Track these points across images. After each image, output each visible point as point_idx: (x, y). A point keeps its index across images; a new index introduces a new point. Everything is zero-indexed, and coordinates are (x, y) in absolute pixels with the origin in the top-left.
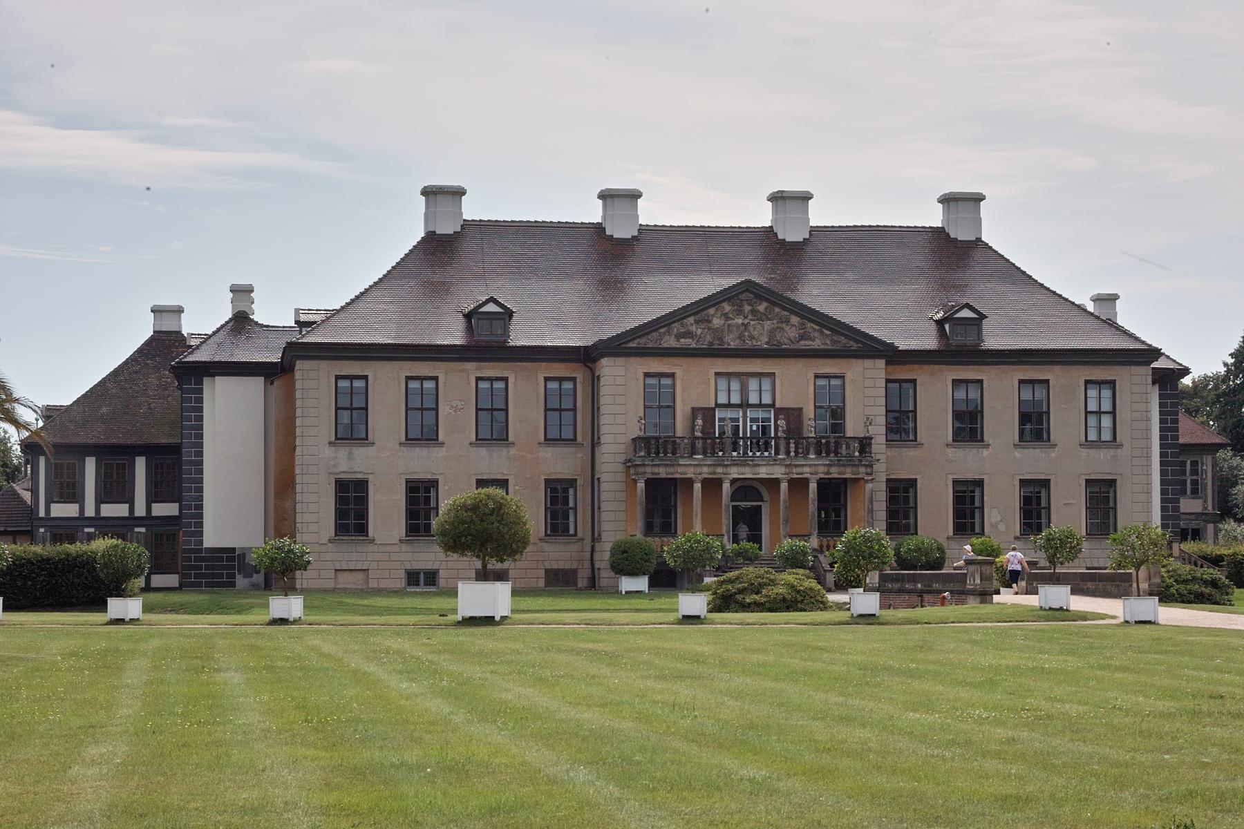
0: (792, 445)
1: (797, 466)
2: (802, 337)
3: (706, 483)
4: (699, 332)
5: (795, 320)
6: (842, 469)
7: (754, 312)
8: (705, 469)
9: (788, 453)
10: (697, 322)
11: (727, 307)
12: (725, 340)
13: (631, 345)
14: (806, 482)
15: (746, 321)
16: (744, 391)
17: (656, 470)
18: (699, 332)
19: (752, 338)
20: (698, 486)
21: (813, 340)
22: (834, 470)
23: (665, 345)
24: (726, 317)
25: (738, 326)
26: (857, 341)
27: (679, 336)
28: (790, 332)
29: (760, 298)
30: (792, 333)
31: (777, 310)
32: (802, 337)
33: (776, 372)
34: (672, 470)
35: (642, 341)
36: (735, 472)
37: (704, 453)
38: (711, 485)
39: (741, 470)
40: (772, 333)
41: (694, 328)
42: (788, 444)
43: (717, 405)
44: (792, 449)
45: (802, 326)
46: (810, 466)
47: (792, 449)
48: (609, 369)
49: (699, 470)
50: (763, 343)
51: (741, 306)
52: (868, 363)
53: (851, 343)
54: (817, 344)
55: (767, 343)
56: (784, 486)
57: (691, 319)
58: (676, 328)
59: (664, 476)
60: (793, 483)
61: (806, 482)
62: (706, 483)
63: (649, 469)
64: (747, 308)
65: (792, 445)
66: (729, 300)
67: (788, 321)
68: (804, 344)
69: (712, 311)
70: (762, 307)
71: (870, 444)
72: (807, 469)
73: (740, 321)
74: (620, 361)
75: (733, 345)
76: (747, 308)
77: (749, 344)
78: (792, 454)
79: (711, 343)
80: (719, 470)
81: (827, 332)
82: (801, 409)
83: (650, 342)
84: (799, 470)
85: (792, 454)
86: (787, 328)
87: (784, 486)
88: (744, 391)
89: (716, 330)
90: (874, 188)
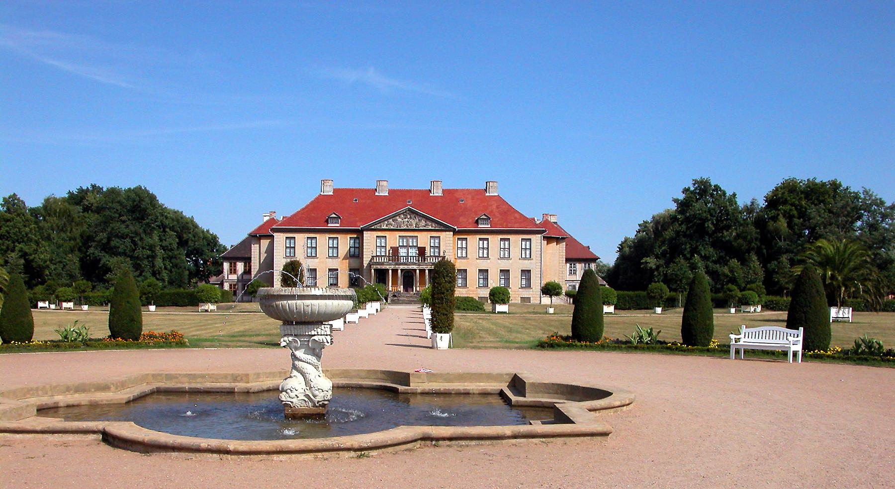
16: (407, 241)
36: (402, 267)
38: (395, 271)
83: (378, 227)
88: (407, 241)
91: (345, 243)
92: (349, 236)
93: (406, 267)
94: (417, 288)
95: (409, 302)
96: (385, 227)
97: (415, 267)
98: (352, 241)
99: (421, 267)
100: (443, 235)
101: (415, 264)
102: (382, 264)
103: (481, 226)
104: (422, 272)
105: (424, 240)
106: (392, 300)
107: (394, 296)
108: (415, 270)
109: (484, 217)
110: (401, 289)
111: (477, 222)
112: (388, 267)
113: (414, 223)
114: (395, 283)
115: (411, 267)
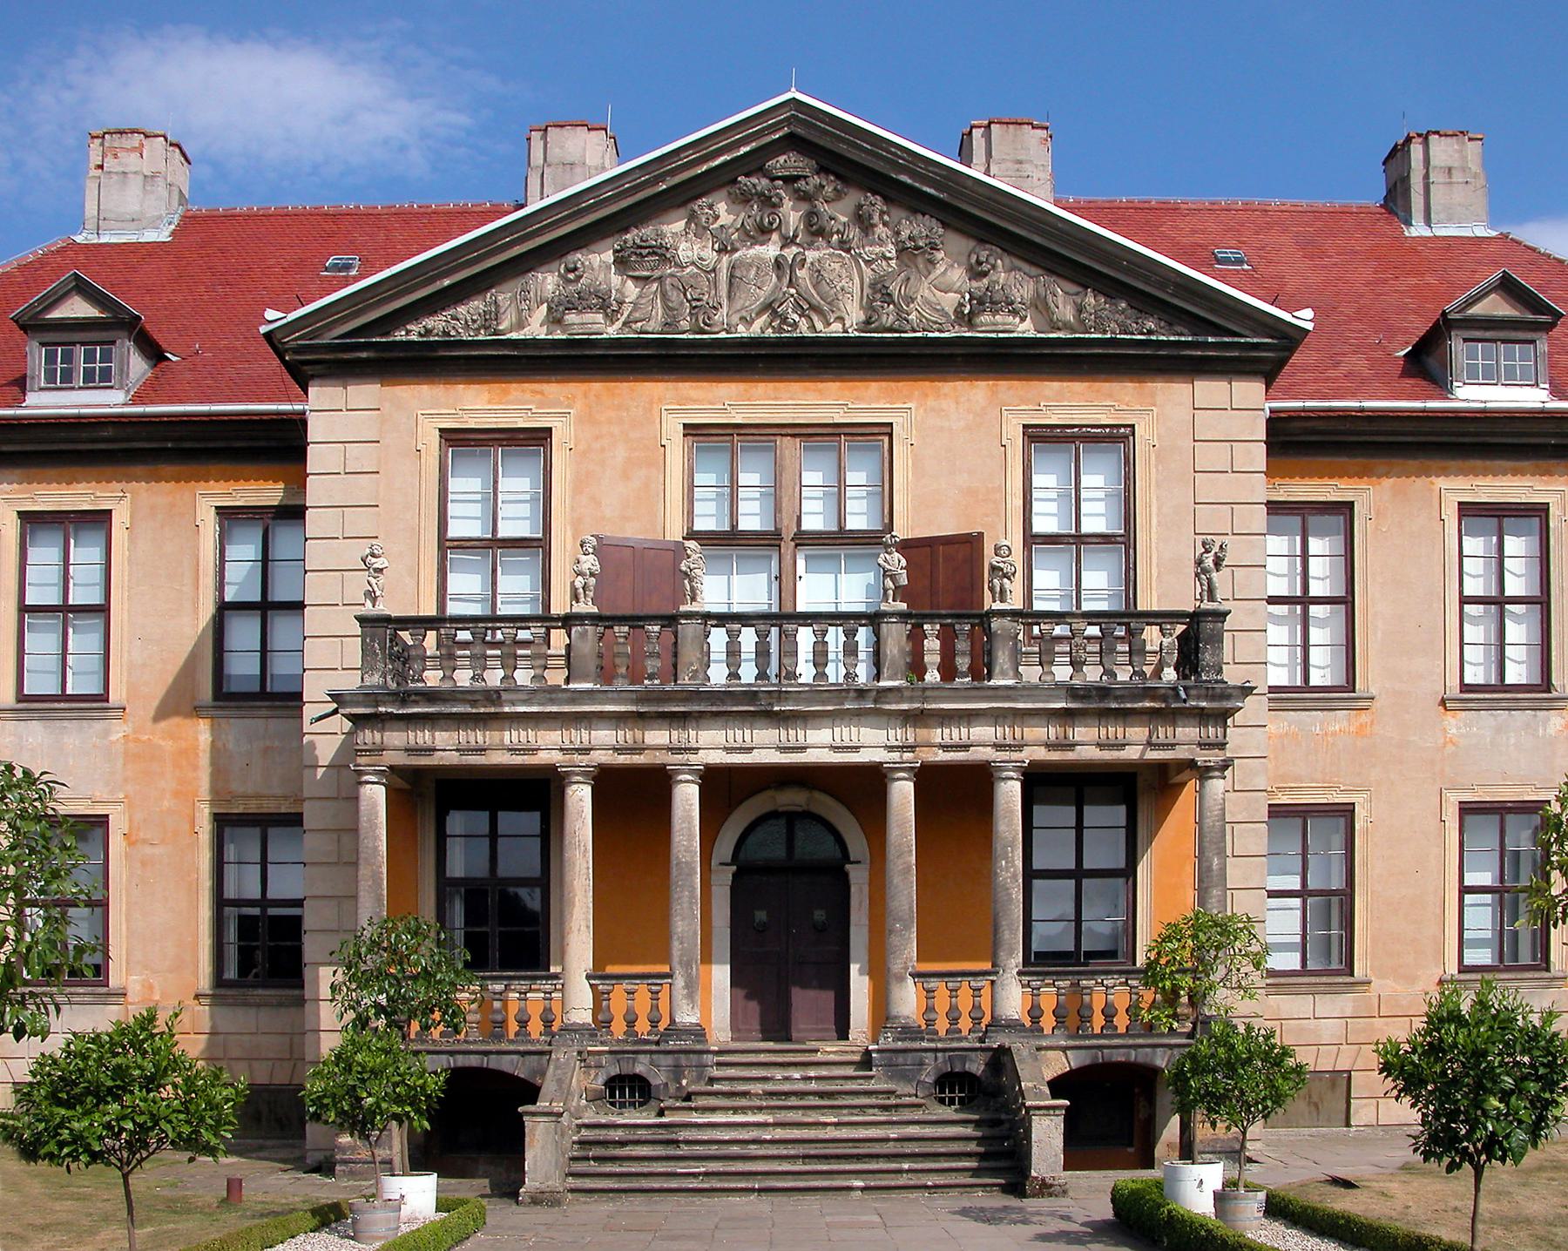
0: (932, 644)
1: (947, 718)
2: (981, 302)
3: (608, 782)
6: (1113, 731)
8: (604, 736)
9: (917, 667)
11: (724, 212)
13: (400, 336)
14: (980, 778)
16: (779, 493)
17: (423, 737)
20: (580, 797)
22: (1081, 733)
28: (939, 293)
33: (897, 421)
34: (479, 737)
36: (714, 745)
37: (605, 673)
38: (632, 798)
39: (740, 735)
42: (916, 637)
43: (692, 535)
44: (932, 658)
46: (996, 717)
47: (932, 658)
48: (337, 415)
49: (580, 736)
52: (1210, 390)
56: (903, 793)
59: (453, 758)
60: (929, 779)
61: (980, 778)
62: (608, 782)
63: (396, 737)
65: (932, 644)
71: (1217, 639)
72: (983, 732)
74: (365, 393)
78: (933, 676)
80: (657, 736)
82: (972, 542)
83: (459, 322)
84: (955, 734)
85: (933, 676)
87: (903, 793)
88: (779, 493)
91: (165, 553)
92: (206, 498)
93: (764, 746)
94: (896, 989)
95: (824, 1169)
96: (536, 328)
97: (871, 744)
98: (245, 551)
99: (941, 745)
100: (1164, 412)
101: (860, 704)
102: (485, 710)
103: (1485, 388)
104: (956, 795)
105: (953, 455)
106: (593, 1151)
107: (628, 1088)
108: (863, 787)
109: (1496, 306)
110: (709, 1000)
111: (1426, 361)
112: (548, 747)
113: (845, 278)
114: (632, 931)
115: (820, 745)
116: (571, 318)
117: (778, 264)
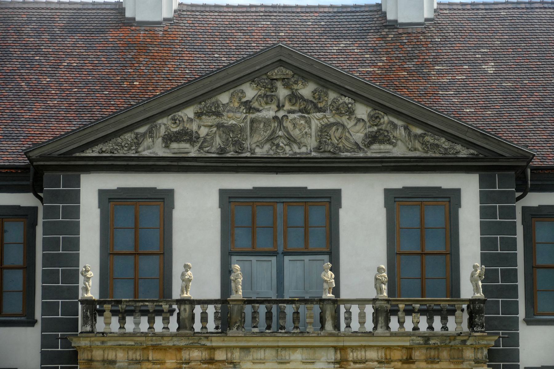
4: (203, 132)
5: (362, 111)
7: (294, 97)
10: (199, 115)
11: (250, 92)
12: (247, 144)
13: (89, 153)
15: (280, 114)
18: (203, 132)
19: (291, 140)
21: (395, 145)
23: (146, 153)
24: (248, 106)
25: (267, 122)
26: (468, 144)
27: (169, 139)
29: (306, 75)
30: (358, 134)
31: (332, 95)
32: (372, 139)
35: (107, 147)
40: (324, 130)
41: (194, 127)
45: (374, 119)
50: (308, 147)
51: (273, 89)
53: (458, 147)
54: (399, 150)
55: (318, 149)
57: (190, 112)
58: (165, 124)
64: (282, 92)
66: (251, 77)
67: (351, 112)
68: (377, 150)
69: (224, 98)
70: (307, 90)
73: (271, 114)
75: (259, 152)
76: (282, 92)
77: (288, 151)
79: (222, 150)
81: (418, 131)
86: (349, 124)
89: (231, 129)
90: (473, 1)
116: (174, 145)
117: (276, 118)
